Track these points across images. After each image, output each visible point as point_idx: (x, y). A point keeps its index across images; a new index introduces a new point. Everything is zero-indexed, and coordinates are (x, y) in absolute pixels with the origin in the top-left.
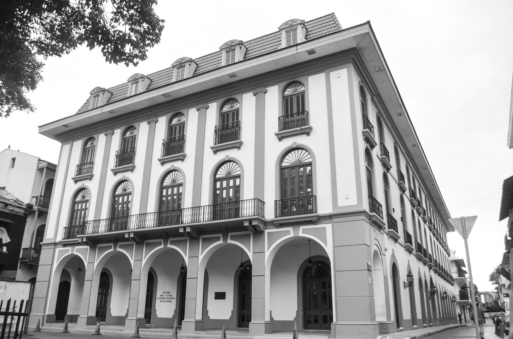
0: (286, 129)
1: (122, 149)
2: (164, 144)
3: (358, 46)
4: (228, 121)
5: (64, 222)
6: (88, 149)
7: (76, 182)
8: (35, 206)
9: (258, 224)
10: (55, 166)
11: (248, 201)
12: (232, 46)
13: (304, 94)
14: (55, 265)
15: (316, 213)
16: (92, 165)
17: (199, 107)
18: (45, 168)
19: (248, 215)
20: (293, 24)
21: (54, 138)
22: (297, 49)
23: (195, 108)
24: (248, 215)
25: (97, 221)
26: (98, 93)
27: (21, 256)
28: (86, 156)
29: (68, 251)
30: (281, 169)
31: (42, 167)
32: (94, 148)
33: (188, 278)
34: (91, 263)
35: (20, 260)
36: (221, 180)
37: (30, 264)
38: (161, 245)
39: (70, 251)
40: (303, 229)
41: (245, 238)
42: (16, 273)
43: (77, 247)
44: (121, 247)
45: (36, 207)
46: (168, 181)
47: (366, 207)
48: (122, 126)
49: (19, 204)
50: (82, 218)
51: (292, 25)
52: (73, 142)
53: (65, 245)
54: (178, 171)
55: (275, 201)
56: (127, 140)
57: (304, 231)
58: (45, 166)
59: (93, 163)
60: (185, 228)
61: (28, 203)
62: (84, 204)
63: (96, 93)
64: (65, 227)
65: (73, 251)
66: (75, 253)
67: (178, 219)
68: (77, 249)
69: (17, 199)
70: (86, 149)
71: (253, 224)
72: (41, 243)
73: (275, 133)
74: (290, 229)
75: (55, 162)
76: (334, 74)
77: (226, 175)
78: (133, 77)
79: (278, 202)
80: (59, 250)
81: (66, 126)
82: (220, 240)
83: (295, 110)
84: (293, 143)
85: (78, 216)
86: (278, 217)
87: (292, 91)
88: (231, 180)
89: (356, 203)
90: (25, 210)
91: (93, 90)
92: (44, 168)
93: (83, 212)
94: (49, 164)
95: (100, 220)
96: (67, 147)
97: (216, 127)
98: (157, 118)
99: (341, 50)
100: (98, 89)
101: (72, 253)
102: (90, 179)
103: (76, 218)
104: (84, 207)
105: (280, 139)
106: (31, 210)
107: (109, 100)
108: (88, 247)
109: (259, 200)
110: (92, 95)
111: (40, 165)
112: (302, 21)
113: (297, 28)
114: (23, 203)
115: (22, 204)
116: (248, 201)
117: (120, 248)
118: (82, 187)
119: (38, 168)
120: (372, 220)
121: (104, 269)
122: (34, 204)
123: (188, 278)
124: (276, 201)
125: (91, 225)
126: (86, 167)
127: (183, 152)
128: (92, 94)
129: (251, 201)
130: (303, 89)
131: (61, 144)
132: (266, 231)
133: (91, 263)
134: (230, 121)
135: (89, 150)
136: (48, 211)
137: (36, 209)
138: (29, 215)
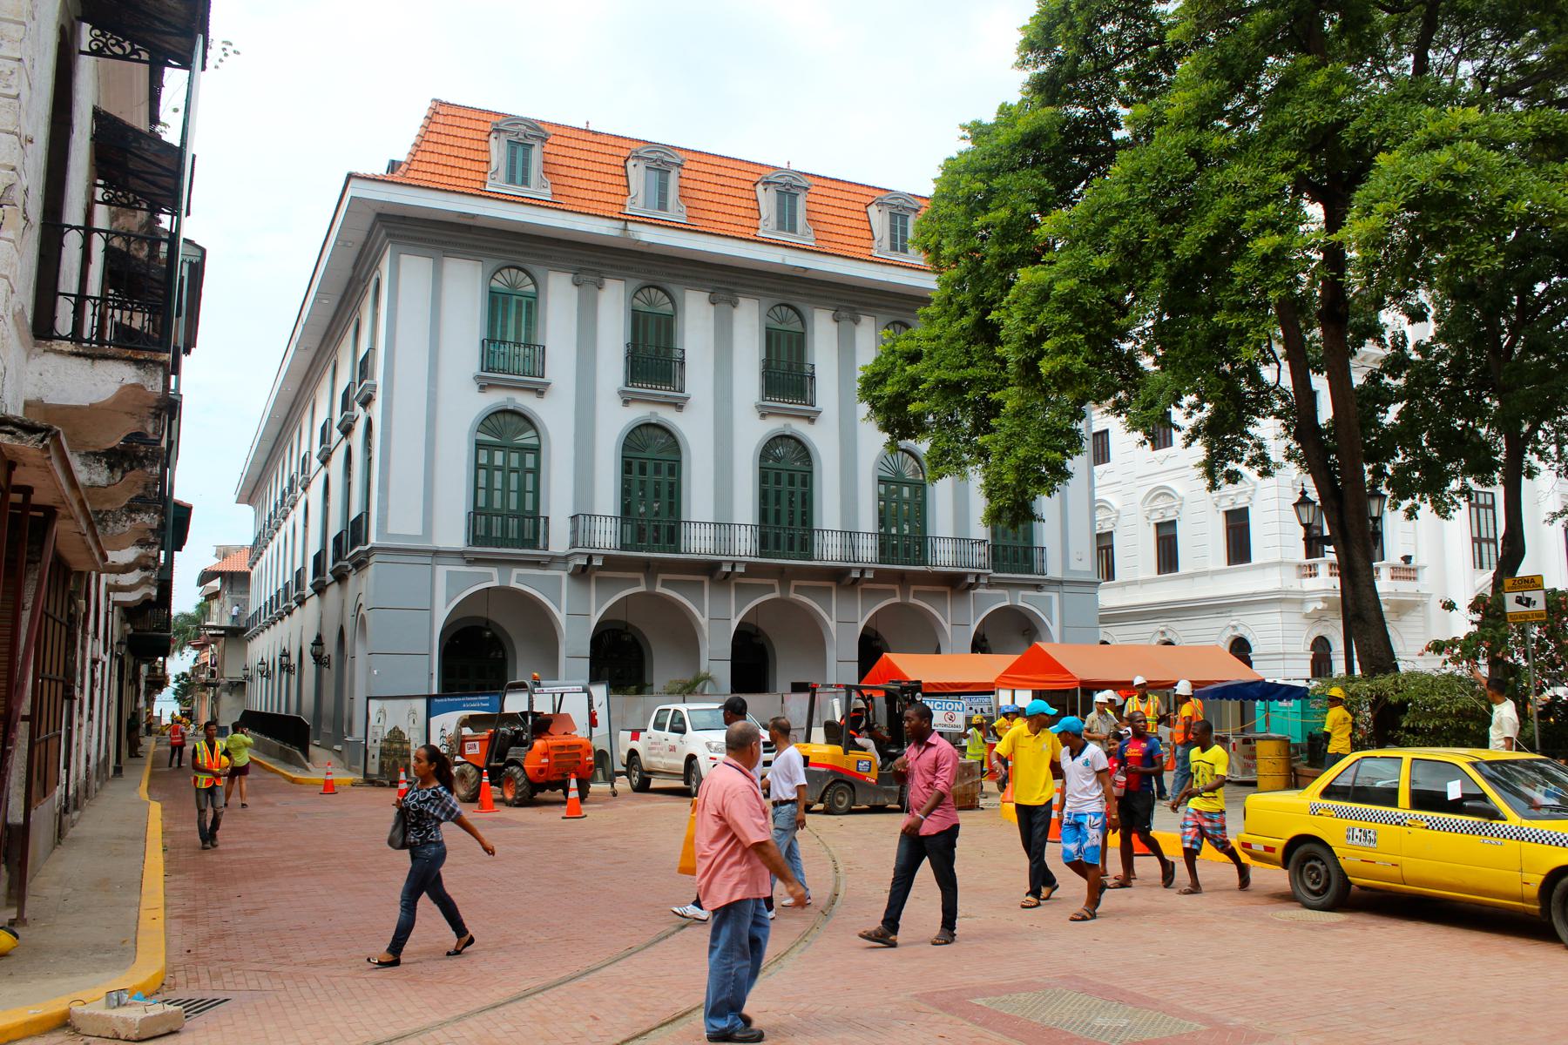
12: (905, 208)
17: (843, 314)
32: (524, 300)
39: (494, 577)
44: (665, 583)
48: (630, 276)
60: (863, 571)
63: (521, 136)
66: (514, 584)
67: (805, 546)
101: (505, 584)
117: (662, 586)
128: (505, 131)
135: (506, 302)
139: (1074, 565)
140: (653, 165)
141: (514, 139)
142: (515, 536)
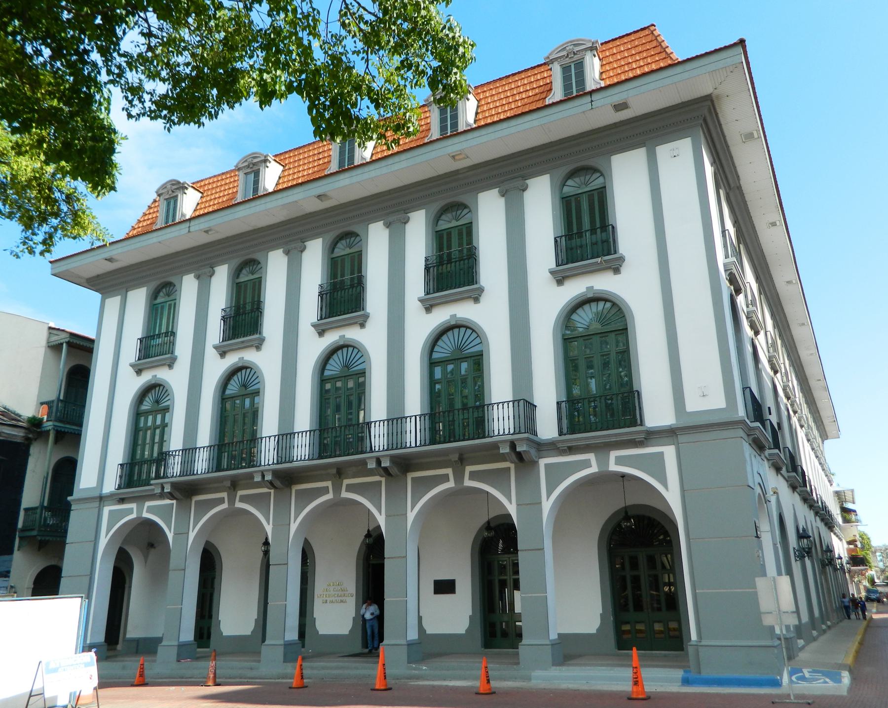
0: (573, 262)
1: (234, 305)
2: (323, 295)
3: (716, 91)
4: (449, 247)
5: (118, 454)
6: (160, 306)
7: (139, 372)
8: (47, 421)
9: (528, 450)
10: (92, 341)
11: (501, 405)
13: (602, 192)
14: (103, 542)
15: (642, 424)
16: (172, 338)
17: (391, 219)
18: (64, 345)
19: (501, 433)
20: (577, 49)
21: (86, 285)
22: (592, 101)
23: (382, 221)
24: (501, 433)
25: (189, 451)
26: (173, 192)
27: (20, 525)
28: (156, 320)
29: (130, 511)
30: (565, 339)
31: (57, 343)
32: (173, 303)
33: (389, 558)
34: (181, 534)
35: (19, 532)
36: (443, 362)
37: (41, 540)
38: (328, 492)
39: (132, 512)
40: (616, 457)
41: (498, 478)
42: (11, 561)
43: (148, 504)
45: (50, 423)
46: (334, 367)
47: (741, 413)
49: (13, 419)
50: (156, 443)
51: (574, 52)
52: (127, 292)
53: (122, 501)
54: (354, 347)
55: (558, 403)
56: (243, 287)
57: (619, 461)
58: (64, 340)
59: (173, 334)
61: (30, 415)
62: (159, 417)
64: (120, 464)
65: (140, 510)
66: (146, 515)
68: (148, 507)
69: (5, 408)
70: (155, 306)
71: (518, 449)
72: (69, 498)
73: (549, 269)
74: (591, 457)
75: (92, 336)
76: (663, 151)
77: (452, 353)
78: (246, 161)
79: (563, 405)
80: (110, 511)
81: (110, 260)
82: (449, 481)
83: (586, 225)
84: (587, 288)
85: (148, 440)
86: (565, 435)
87: (577, 186)
88: (462, 364)
89: (723, 405)
90: (26, 431)
91: (164, 186)
92: (62, 344)
93: (158, 431)
94: (73, 335)
95: (196, 449)
96: (114, 303)
97: (427, 260)
98: (304, 242)
99: (680, 102)
100: (173, 185)
101: (139, 516)
102: (170, 366)
103: (144, 444)
104: (158, 422)
105: (560, 282)
106: (39, 430)
107: (196, 207)
108: (174, 502)
109: (526, 401)
110: (161, 197)
111: (54, 338)
112: (593, 43)
113: (584, 58)
114: (20, 416)
115: (19, 418)
116: (501, 405)
118: (153, 382)
119: (50, 344)
120: (753, 436)
121: (207, 541)
122: (45, 417)
123: (389, 558)
124: (559, 404)
125: (178, 459)
126: (159, 341)
127: (363, 310)
129: (506, 405)
130: (601, 180)
131: (100, 295)
132: (543, 462)
133: (181, 534)
134: (455, 247)
135: (162, 308)
136: (81, 431)
137: (50, 428)
138: (36, 440)
139: (694, 404)
140: (249, 170)
141: (167, 197)
142: (144, 478)
